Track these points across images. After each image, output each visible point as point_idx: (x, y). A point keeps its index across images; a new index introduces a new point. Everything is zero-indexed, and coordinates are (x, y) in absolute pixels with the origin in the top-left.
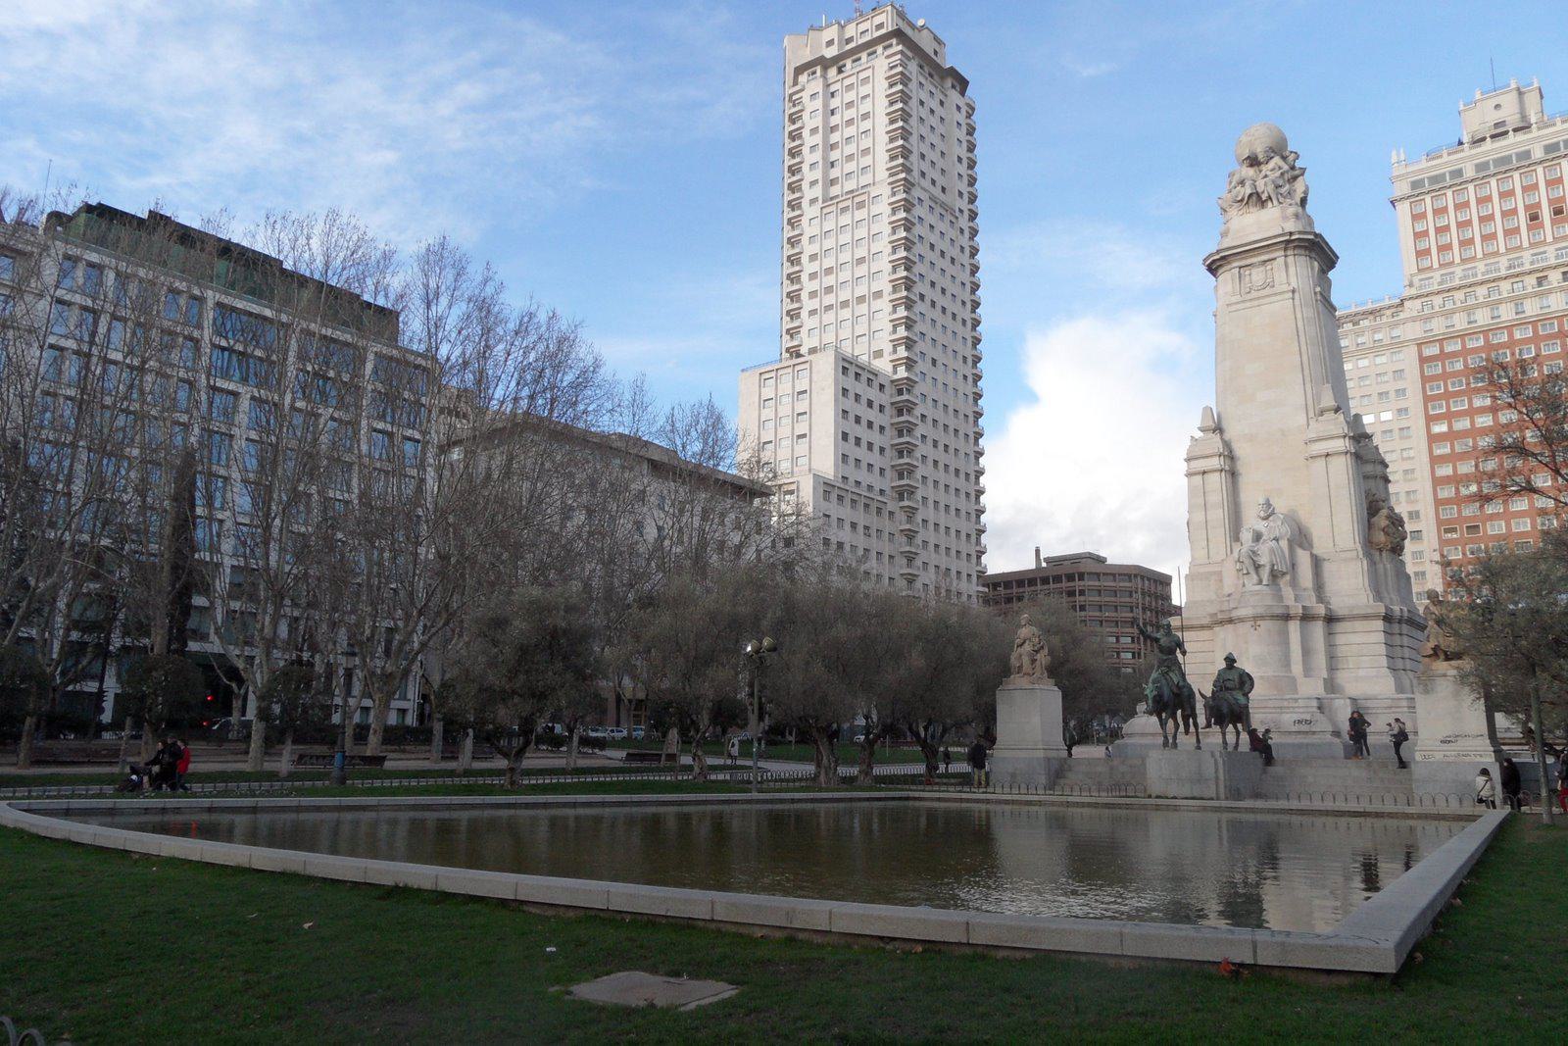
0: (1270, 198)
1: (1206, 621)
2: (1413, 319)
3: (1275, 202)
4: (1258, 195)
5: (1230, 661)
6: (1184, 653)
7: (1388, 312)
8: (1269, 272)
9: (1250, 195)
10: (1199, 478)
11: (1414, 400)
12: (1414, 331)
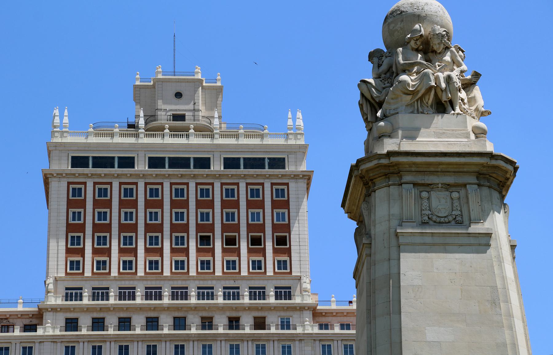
2: (54, 340)
8: (456, 204)
9: (431, 87)
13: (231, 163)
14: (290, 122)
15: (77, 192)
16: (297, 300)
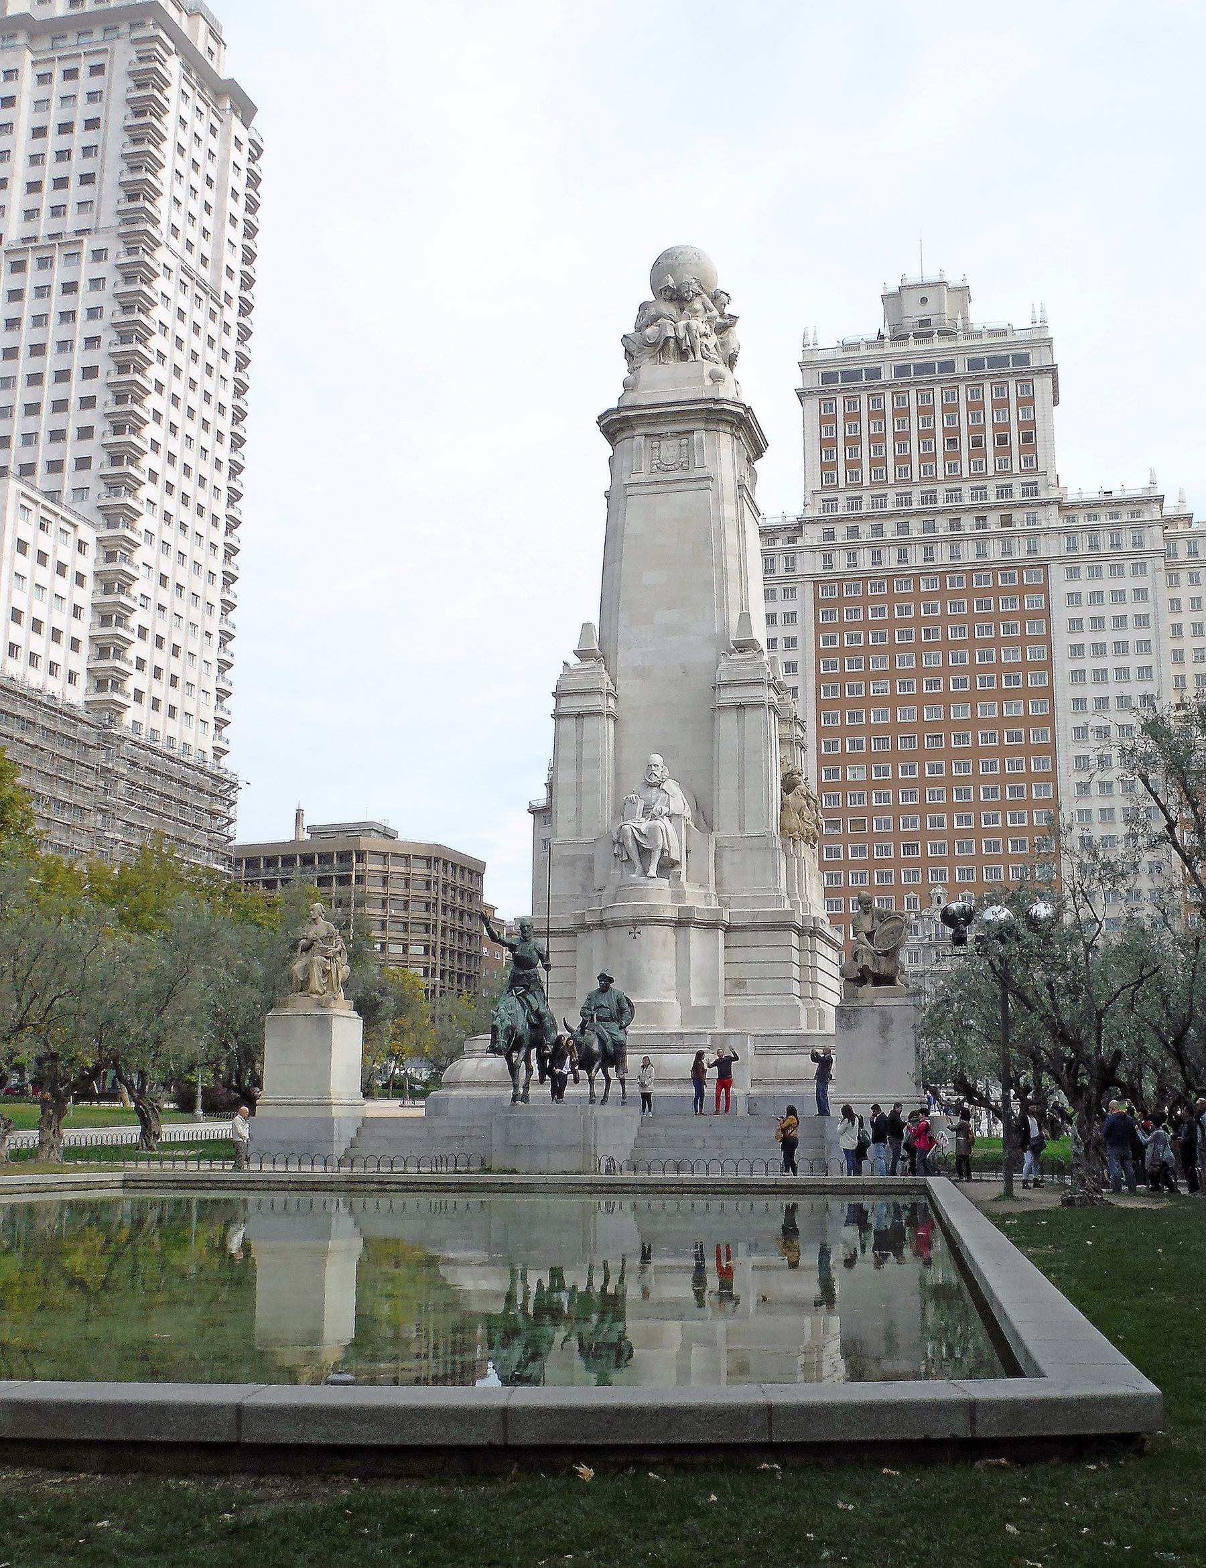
1: (566, 925)
2: (812, 549)
3: (699, 356)
5: (606, 981)
6: (547, 968)
7: (784, 536)
9: (668, 338)
10: (569, 725)
12: (809, 564)
13: (975, 364)
15: (829, 407)
16: (1043, 495)
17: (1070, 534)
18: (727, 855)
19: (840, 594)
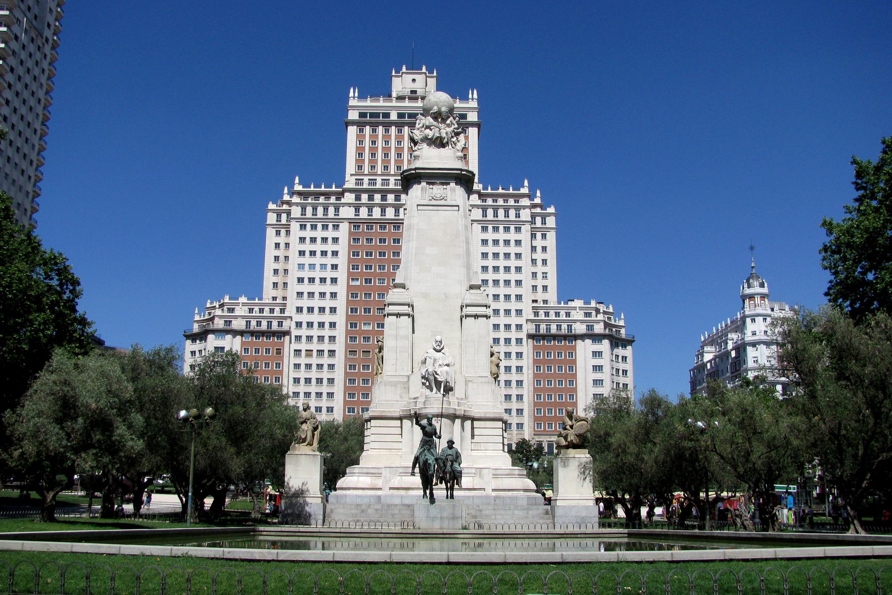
0: (447, 143)
2: (349, 205)
4: (441, 138)
5: (451, 443)
11: (342, 261)
12: (347, 212)
14: (470, 96)
15: (361, 131)
17: (485, 210)
18: (470, 384)
19: (363, 230)
